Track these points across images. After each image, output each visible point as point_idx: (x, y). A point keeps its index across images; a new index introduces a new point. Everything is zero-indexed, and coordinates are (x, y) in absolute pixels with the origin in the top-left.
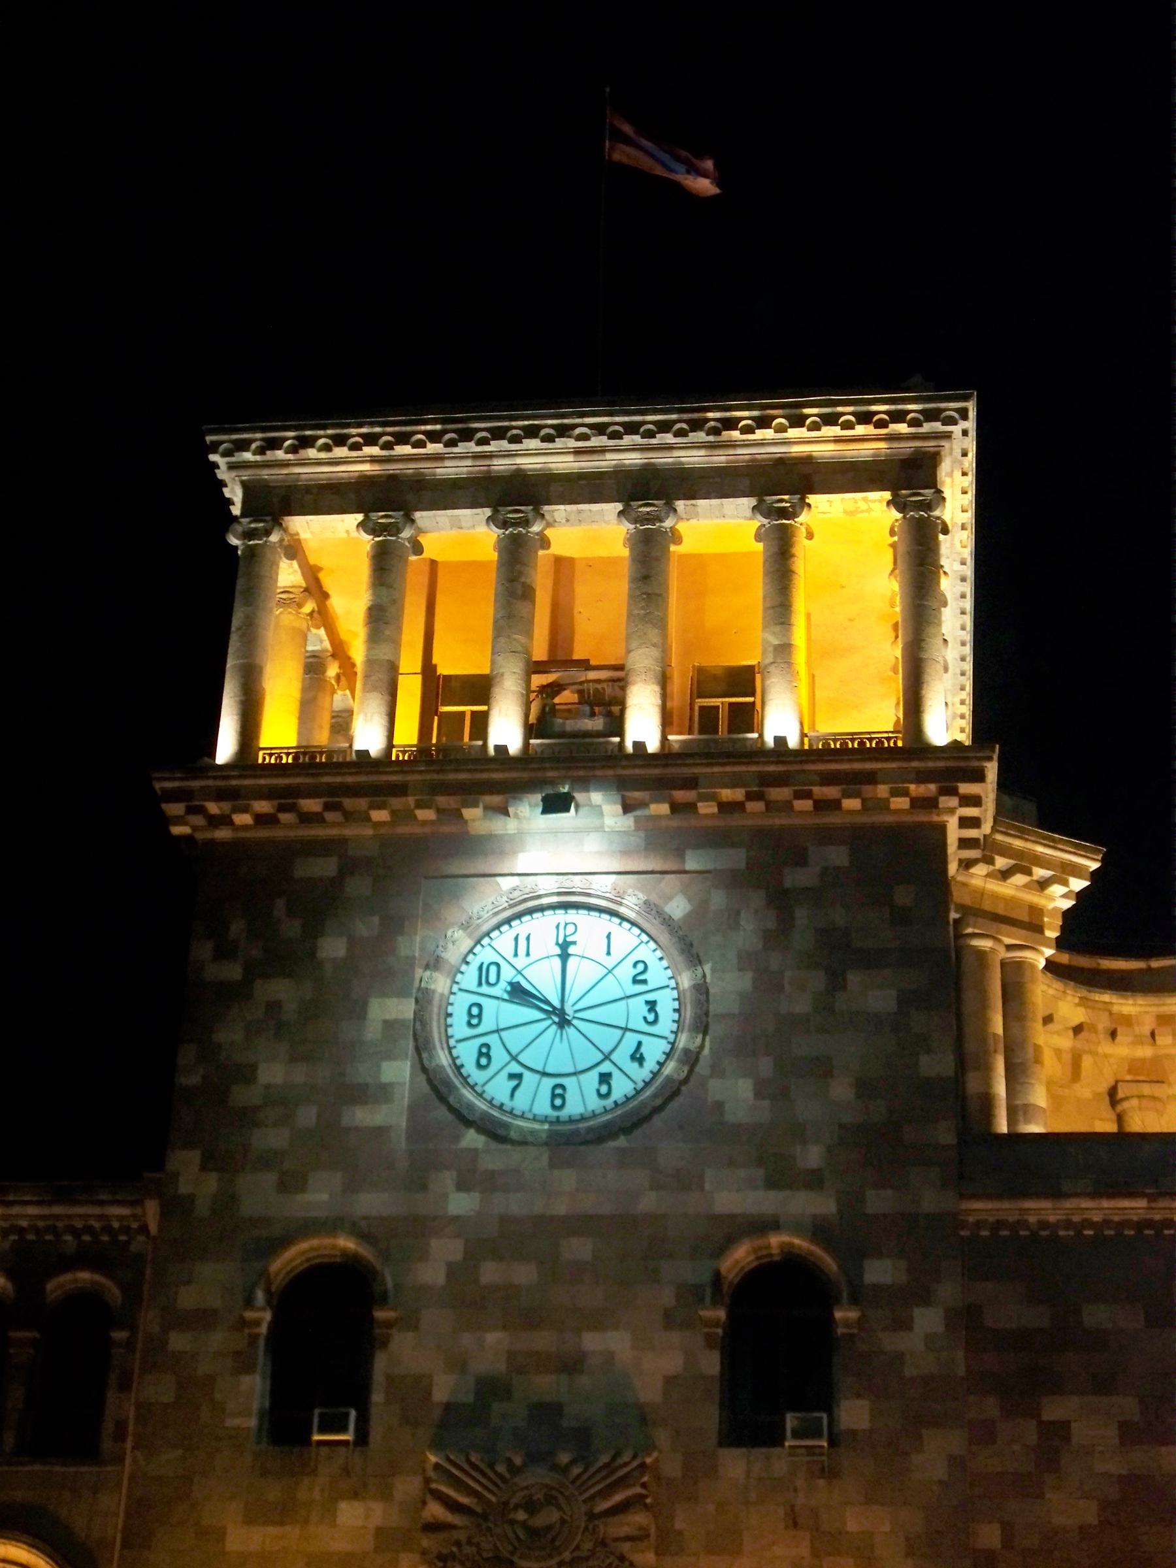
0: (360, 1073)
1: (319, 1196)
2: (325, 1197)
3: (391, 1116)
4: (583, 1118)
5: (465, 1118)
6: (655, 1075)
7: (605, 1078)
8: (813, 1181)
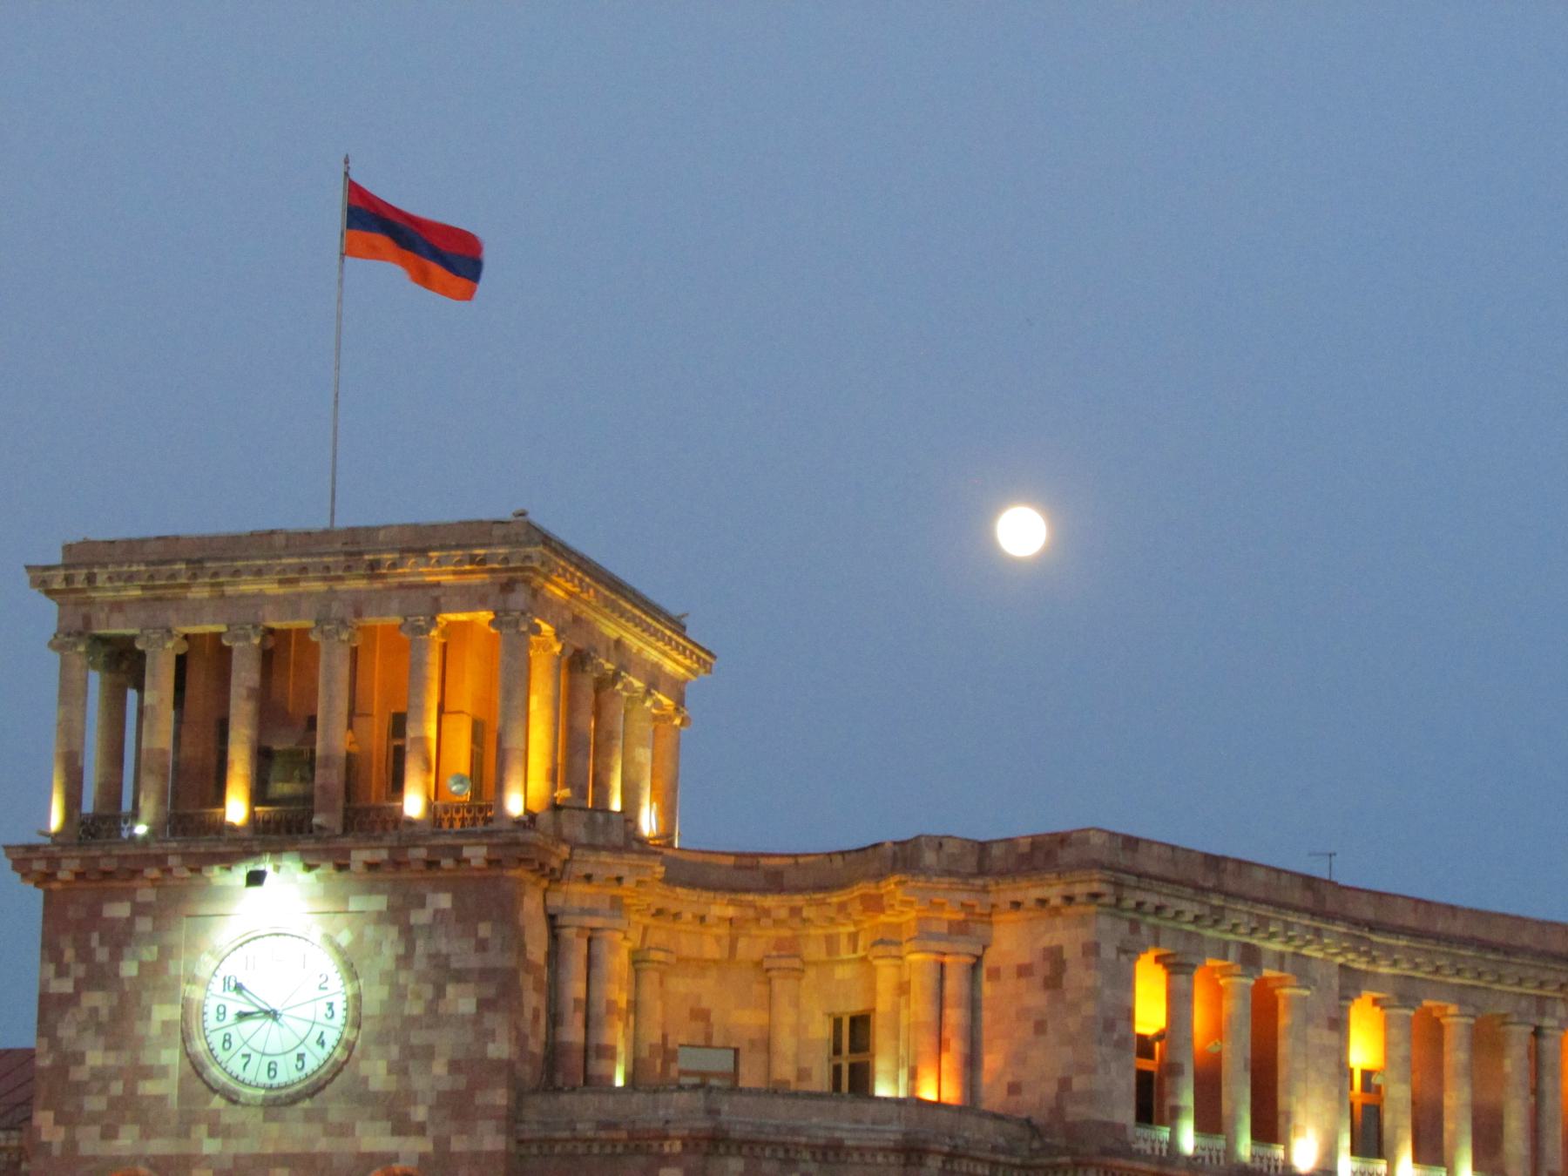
0: (147, 1058)
1: (127, 1141)
2: (129, 1142)
3: (165, 1088)
4: (286, 1086)
5: (213, 1089)
6: (331, 1055)
7: (301, 1057)
8: (421, 1129)
